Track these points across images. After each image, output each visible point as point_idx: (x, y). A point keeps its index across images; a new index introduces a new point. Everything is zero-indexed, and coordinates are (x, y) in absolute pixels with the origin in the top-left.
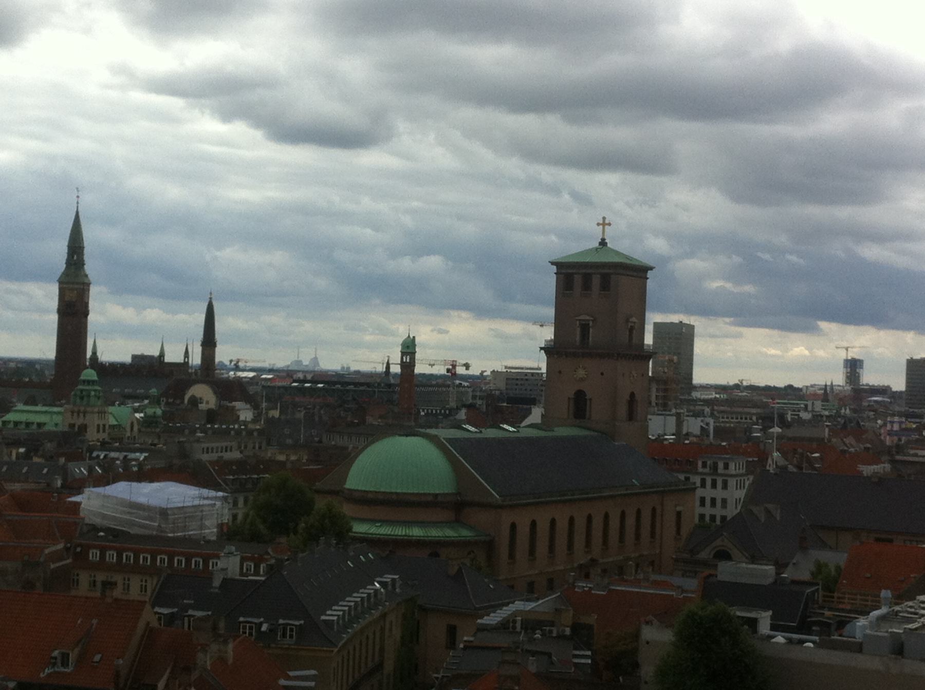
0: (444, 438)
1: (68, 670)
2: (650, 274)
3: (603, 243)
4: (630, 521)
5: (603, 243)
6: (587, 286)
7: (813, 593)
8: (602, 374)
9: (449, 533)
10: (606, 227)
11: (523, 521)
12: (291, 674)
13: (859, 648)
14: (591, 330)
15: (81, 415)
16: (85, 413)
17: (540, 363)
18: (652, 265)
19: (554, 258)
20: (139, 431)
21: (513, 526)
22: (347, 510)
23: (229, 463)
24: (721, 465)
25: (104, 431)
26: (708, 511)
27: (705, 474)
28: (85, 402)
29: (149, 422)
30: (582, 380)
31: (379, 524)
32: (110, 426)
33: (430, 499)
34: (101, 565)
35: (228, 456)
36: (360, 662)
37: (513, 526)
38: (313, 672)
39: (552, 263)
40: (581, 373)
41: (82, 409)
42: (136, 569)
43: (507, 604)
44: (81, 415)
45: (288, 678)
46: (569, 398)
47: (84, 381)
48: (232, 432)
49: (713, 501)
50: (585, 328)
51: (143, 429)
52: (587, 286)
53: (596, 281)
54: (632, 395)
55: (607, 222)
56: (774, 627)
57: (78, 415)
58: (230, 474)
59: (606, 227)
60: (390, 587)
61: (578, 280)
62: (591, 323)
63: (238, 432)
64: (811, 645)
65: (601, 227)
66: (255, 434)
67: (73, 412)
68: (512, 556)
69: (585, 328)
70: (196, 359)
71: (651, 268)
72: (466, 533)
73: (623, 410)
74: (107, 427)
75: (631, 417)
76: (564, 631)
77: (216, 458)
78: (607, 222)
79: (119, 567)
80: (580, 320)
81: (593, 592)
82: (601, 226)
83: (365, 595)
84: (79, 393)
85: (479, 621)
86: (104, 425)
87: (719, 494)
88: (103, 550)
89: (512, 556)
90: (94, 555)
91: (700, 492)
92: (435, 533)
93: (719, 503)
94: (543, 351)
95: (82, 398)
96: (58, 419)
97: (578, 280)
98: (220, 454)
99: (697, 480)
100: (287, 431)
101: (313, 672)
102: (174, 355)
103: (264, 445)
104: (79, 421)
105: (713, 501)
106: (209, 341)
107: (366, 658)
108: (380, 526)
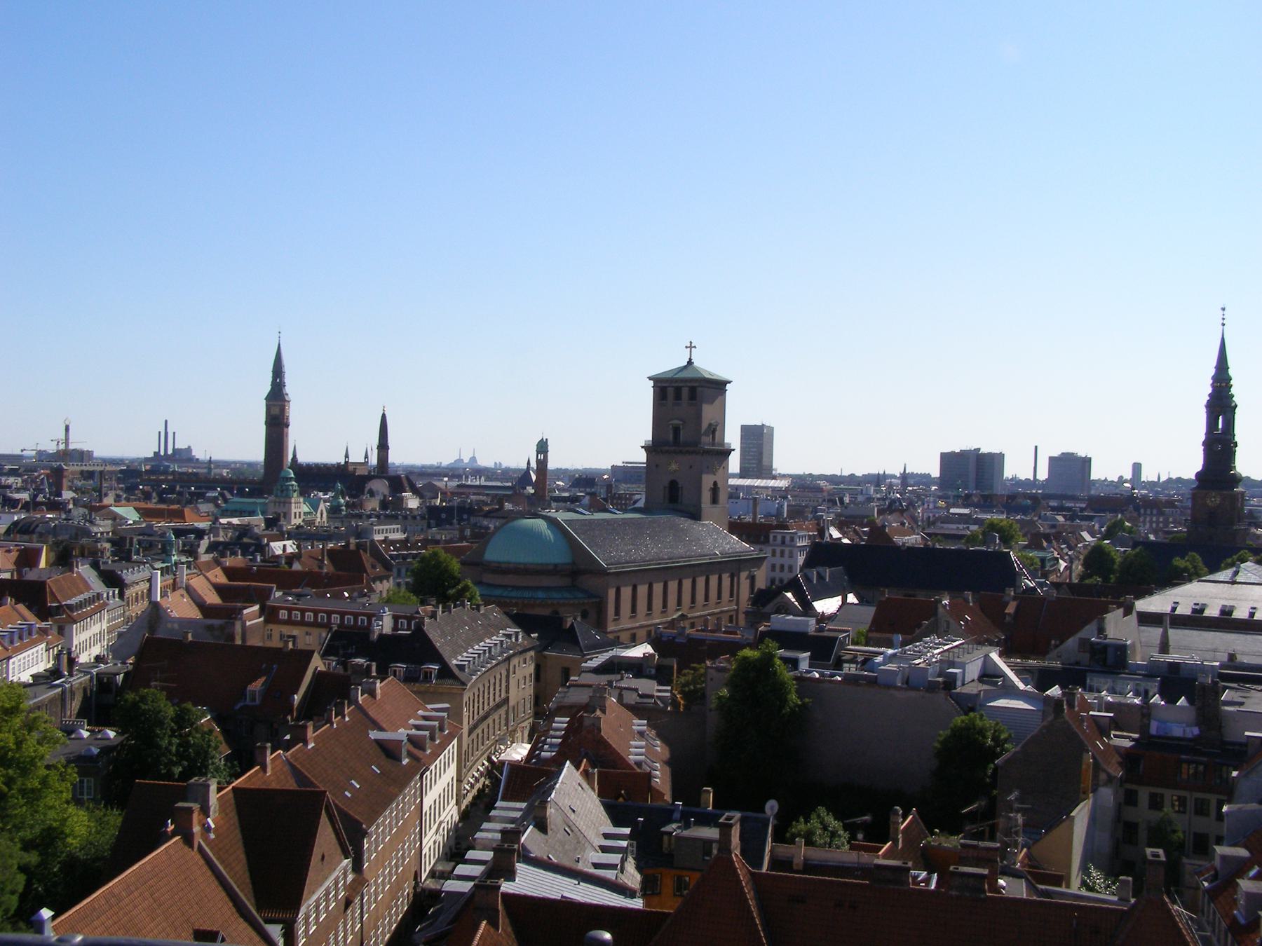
0: (565, 521)
2: (728, 385)
3: (690, 362)
5: (690, 362)
6: (678, 396)
7: (845, 637)
8: (691, 467)
10: (693, 349)
12: (429, 706)
14: (681, 432)
15: (282, 505)
16: (284, 503)
17: (641, 457)
18: (731, 380)
19: (650, 375)
20: (328, 517)
23: (393, 542)
24: (788, 538)
25: (300, 517)
27: (775, 546)
28: (284, 495)
30: (675, 471)
31: (509, 589)
32: (305, 513)
33: (551, 567)
34: (290, 622)
35: (393, 536)
36: (479, 696)
38: (447, 705)
39: (650, 378)
40: (674, 467)
41: (282, 500)
42: (315, 624)
43: (608, 651)
44: (282, 505)
45: (427, 710)
46: (665, 487)
47: (283, 478)
48: (400, 517)
49: (782, 567)
50: (676, 430)
51: (331, 515)
52: (678, 396)
53: (685, 393)
54: (715, 483)
55: (693, 345)
57: (279, 505)
58: (393, 551)
59: (693, 349)
60: (513, 640)
61: (671, 392)
62: (681, 427)
64: (839, 679)
65: (689, 349)
66: (418, 517)
67: (275, 502)
68: (617, 612)
69: (676, 430)
70: (374, 460)
71: (729, 382)
74: (302, 514)
76: (650, 671)
77: (383, 538)
78: (693, 345)
80: (672, 424)
81: (677, 640)
82: (689, 349)
83: (487, 648)
84: (279, 487)
85: (583, 664)
86: (300, 513)
87: (786, 561)
88: (290, 610)
89: (617, 612)
90: (283, 614)
93: (786, 568)
94: (643, 450)
95: (282, 491)
97: (671, 392)
98: (386, 535)
100: (444, 516)
101: (447, 705)
102: (356, 457)
103: (425, 527)
105: (782, 567)
106: (383, 446)
107: (494, 694)
108: (511, 591)
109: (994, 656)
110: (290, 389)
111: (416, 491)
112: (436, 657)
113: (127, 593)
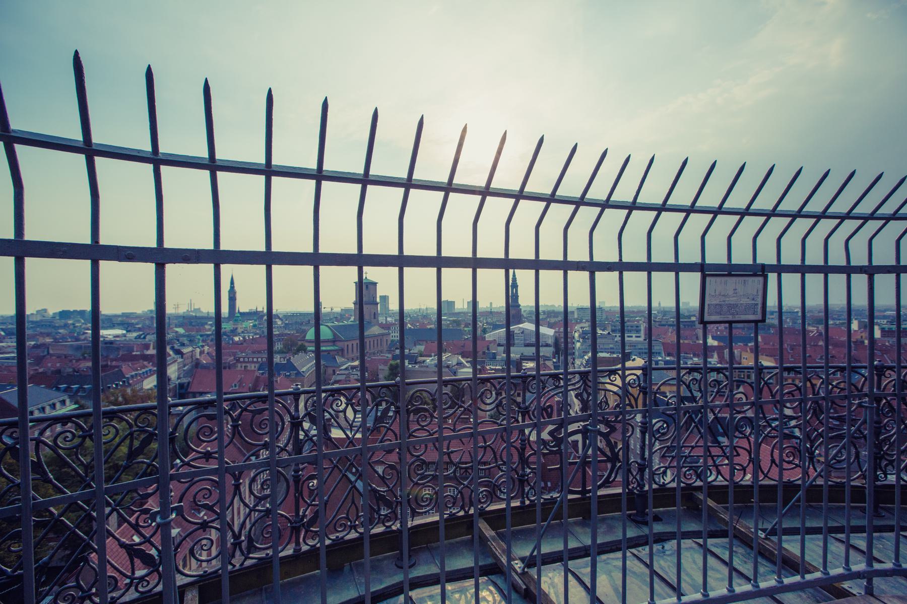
1: (237, 388)
4: (376, 342)
9: (332, 348)
11: (350, 344)
13: (427, 367)
21: (348, 346)
22: (306, 344)
26: (393, 338)
29: (254, 326)
34: (244, 362)
37: (348, 346)
42: (253, 362)
56: (409, 364)
63: (278, 327)
68: (348, 352)
72: (336, 348)
73: (373, 317)
75: (375, 318)
79: (248, 362)
88: (244, 358)
89: (348, 352)
90: (242, 360)
91: (392, 334)
92: (329, 348)
96: (230, 326)
99: (391, 332)
102: (260, 309)
104: (235, 327)
109: (460, 358)
110: (236, 288)
111: (279, 318)
112: (295, 368)
113: (184, 356)
